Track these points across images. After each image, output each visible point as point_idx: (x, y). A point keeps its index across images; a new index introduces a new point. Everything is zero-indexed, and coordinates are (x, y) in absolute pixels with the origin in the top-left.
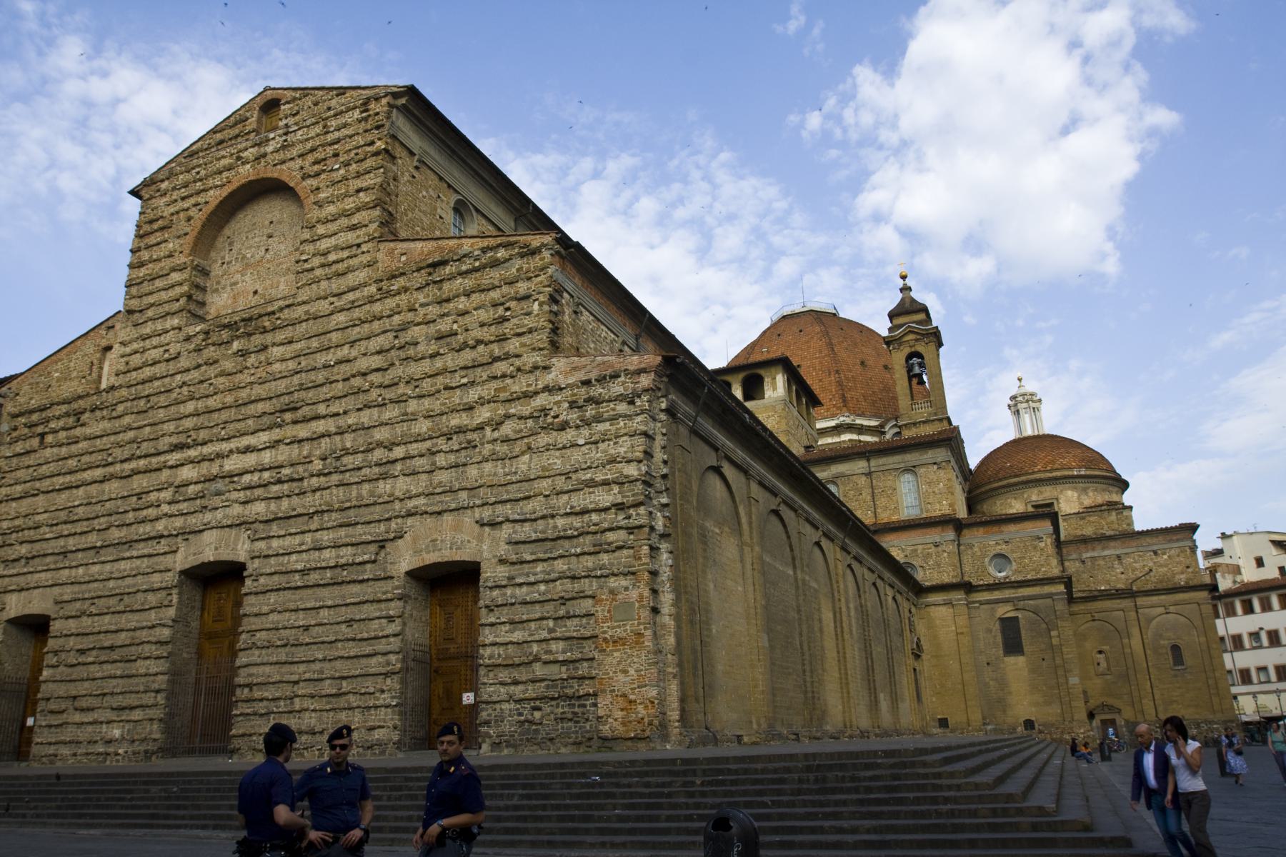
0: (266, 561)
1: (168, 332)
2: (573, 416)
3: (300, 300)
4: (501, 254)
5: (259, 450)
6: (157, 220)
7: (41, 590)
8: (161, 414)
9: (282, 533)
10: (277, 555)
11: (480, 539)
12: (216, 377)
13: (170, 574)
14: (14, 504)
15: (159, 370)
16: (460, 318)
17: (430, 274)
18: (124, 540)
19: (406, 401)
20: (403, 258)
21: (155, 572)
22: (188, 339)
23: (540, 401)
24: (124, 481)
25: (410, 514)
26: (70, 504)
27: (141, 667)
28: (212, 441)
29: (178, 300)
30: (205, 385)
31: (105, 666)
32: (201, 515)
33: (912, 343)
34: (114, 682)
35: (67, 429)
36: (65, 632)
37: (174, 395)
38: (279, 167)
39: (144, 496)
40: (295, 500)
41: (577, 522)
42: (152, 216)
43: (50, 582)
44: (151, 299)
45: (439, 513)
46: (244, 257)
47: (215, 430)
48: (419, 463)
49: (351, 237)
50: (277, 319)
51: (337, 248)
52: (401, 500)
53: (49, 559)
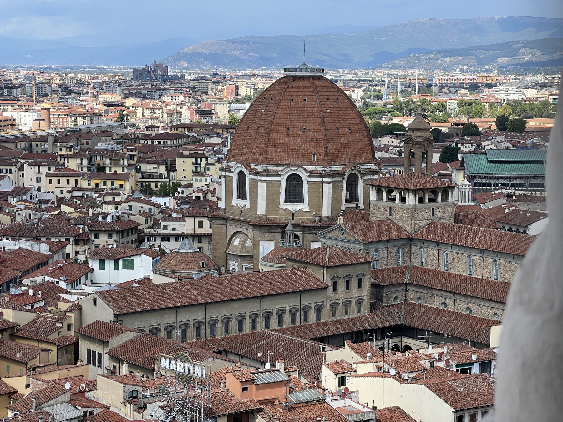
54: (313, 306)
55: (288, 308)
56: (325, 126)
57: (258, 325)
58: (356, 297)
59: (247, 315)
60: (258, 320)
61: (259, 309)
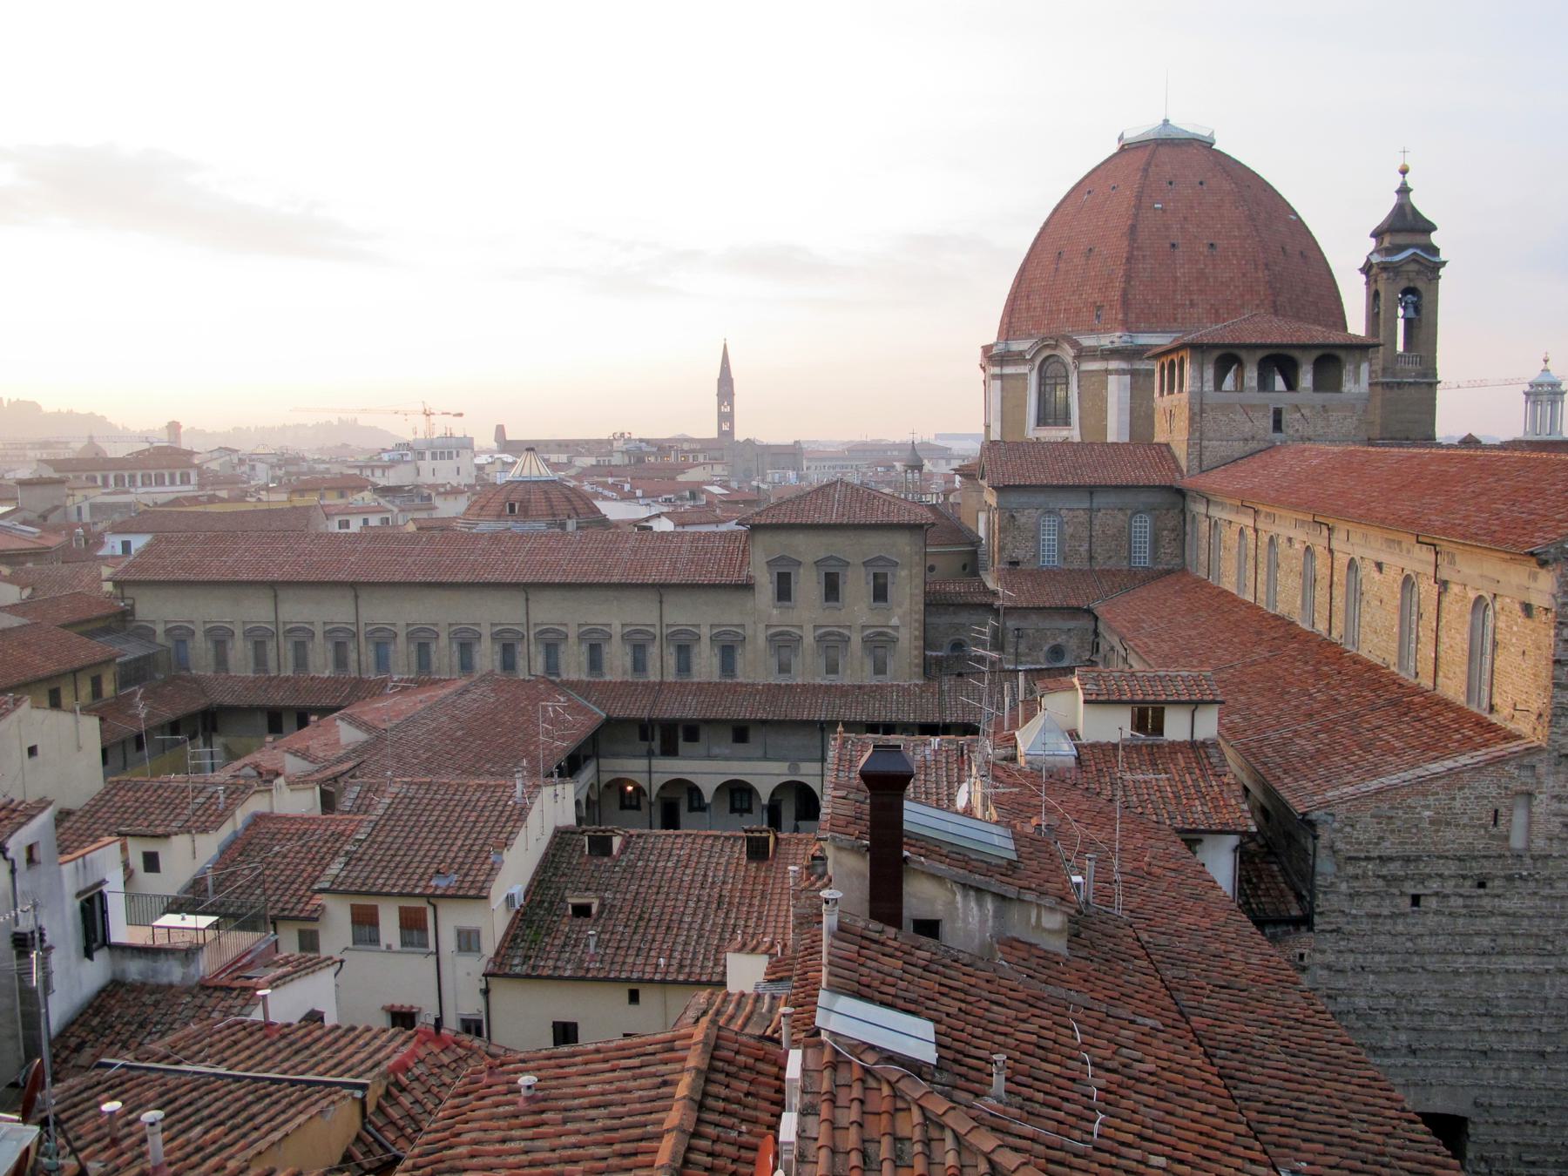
33: (1412, 275)
54: (705, 632)
55: (616, 630)
56: (1134, 240)
57: (521, 663)
58: (864, 627)
59: (486, 631)
60: (521, 649)
61: (524, 621)
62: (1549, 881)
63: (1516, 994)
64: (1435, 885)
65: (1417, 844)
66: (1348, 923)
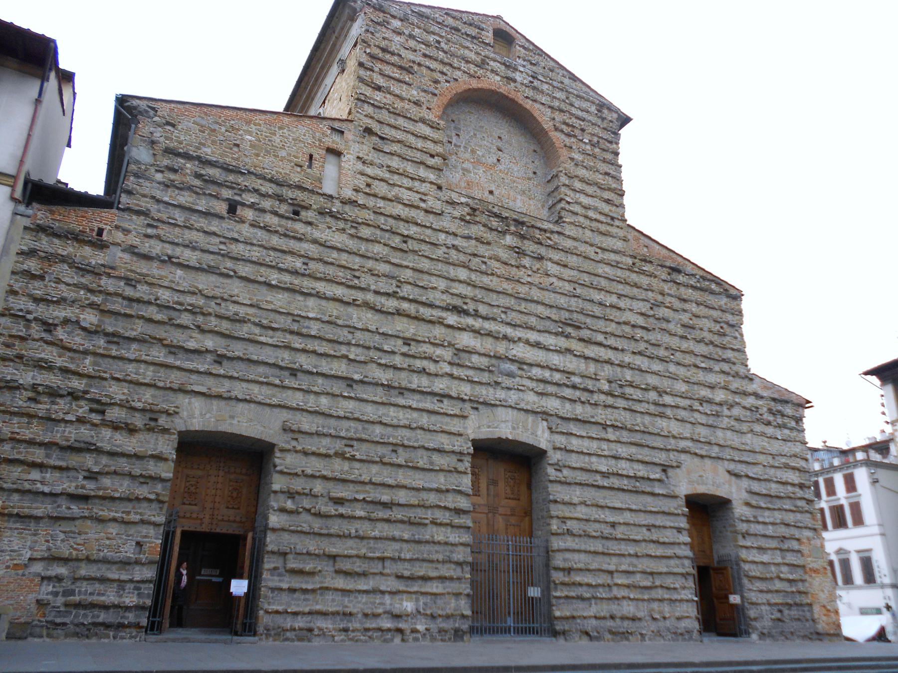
0: (568, 455)
1: (424, 182)
2: (771, 418)
3: (567, 233)
4: (713, 286)
5: (549, 350)
6: (393, 54)
7: (252, 405)
8: (425, 264)
9: (584, 434)
10: (582, 453)
11: (730, 485)
12: (491, 258)
13: (459, 438)
14: (179, 272)
15: (420, 216)
16: (694, 318)
17: (669, 274)
18: (396, 384)
19: (667, 362)
20: (645, 249)
21: (442, 432)
22: (452, 203)
23: (750, 401)
24: (382, 316)
25: (684, 451)
26: (303, 314)
27: (440, 535)
28: (494, 319)
29: (432, 156)
30: (477, 260)
31: (380, 525)
32: (491, 390)
34: (396, 546)
35: (282, 216)
36: (309, 471)
37: (440, 252)
38: (531, 102)
39: (412, 343)
40: (588, 408)
41: (781, 488)
42: (383, 44)
43: (275, 401)
44: (399, 135)
45: (702, 457)
46: (473, 152)
47: (495, 310)
48: (683, 414)
49: (606, 208)
50: (549, 238)
51: (596, 209)
52: (674, 437)
53: (261, 369)
62: (356, 224)
63: (326, 318)
64: (250, 199)
65: (237, 159)
66: (159, 211)
